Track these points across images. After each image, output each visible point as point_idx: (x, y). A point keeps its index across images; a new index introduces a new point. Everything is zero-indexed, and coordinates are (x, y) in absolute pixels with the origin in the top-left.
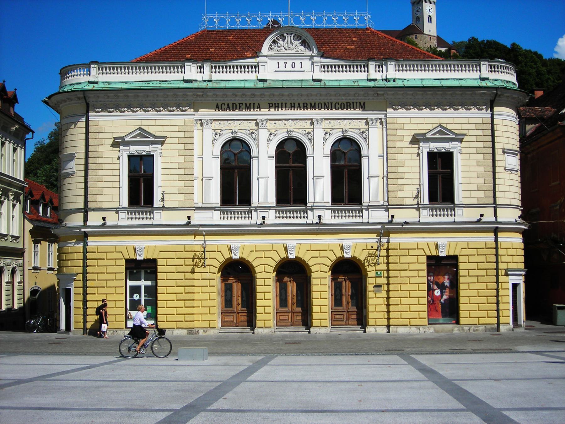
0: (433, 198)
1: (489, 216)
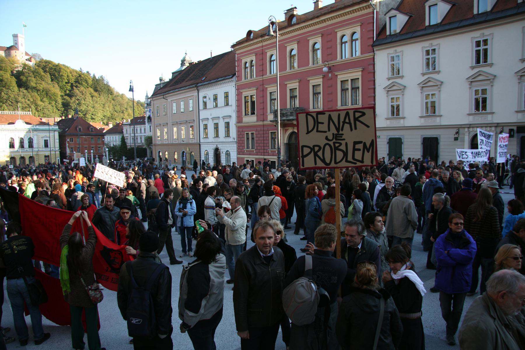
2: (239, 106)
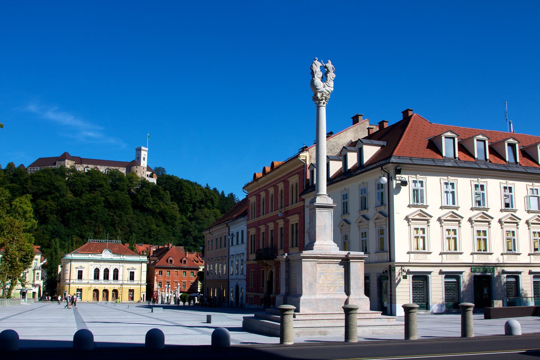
0: (130, 279)
1: (140, 283)
2: (248, 244)
